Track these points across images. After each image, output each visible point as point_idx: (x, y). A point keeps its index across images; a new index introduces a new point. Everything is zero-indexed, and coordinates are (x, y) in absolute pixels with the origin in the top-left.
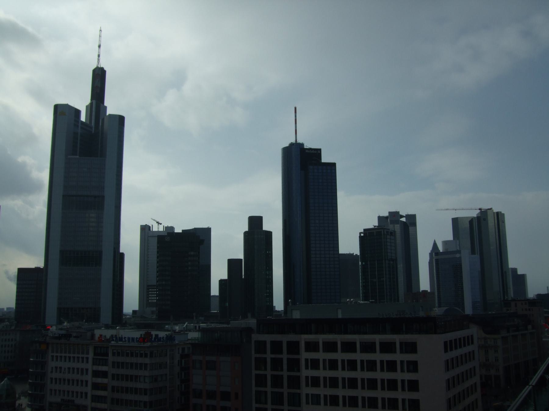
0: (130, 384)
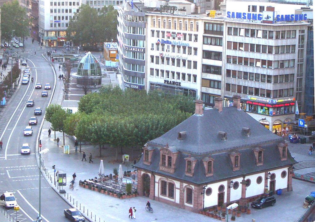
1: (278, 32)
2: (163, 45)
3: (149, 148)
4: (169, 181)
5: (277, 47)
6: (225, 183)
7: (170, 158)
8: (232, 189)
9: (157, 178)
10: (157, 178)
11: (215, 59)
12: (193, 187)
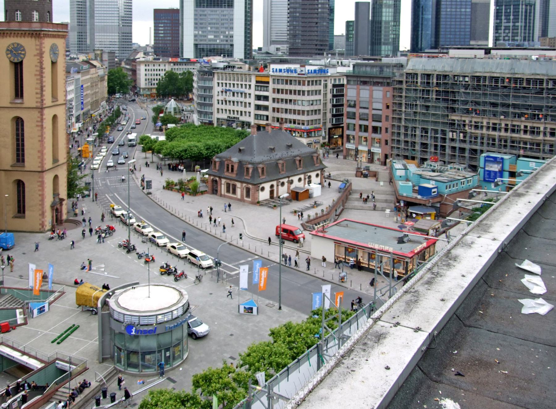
0: (289, 106)
1: (309, 82)
2: (226, 92)
3: (217, 160)
4: (232, 182)
5: (308, 91)
6: (275, 183)
7: (232, 166)
8: (280, 187)
9: (223, 181)
10: (223, 181)
11: (264, 100)
12: (250, 186)
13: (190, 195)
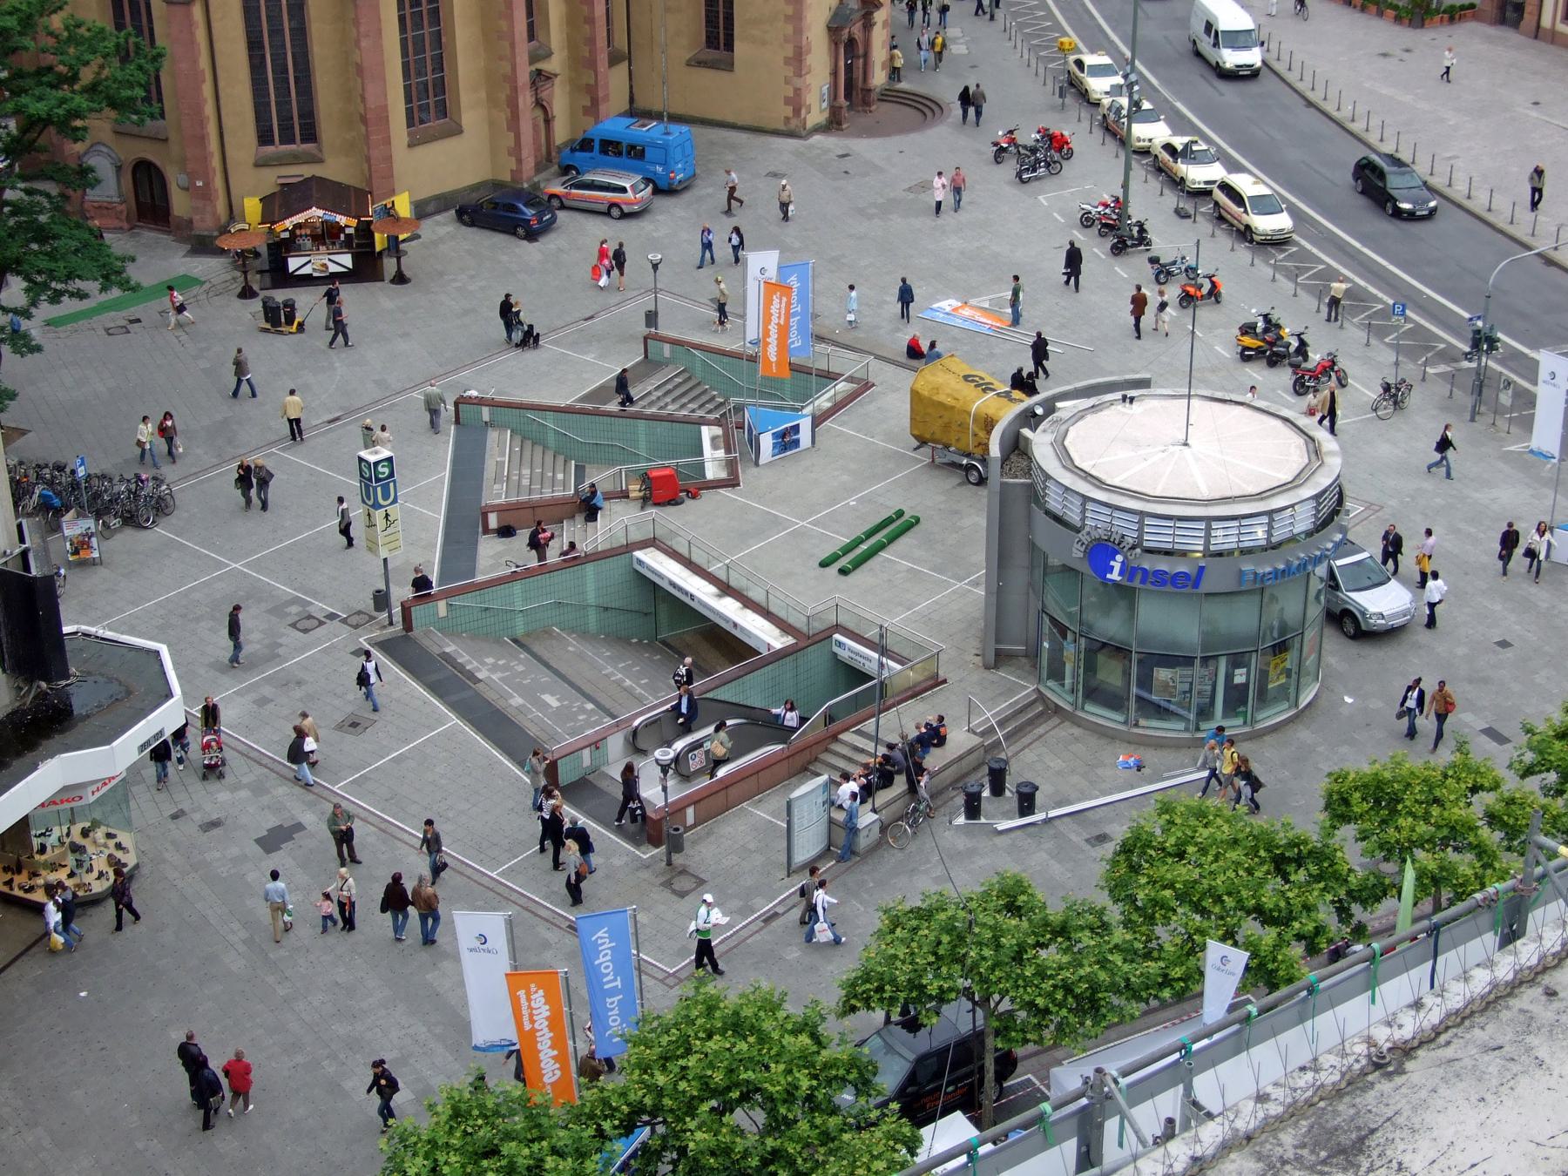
13: (1398, 19)
